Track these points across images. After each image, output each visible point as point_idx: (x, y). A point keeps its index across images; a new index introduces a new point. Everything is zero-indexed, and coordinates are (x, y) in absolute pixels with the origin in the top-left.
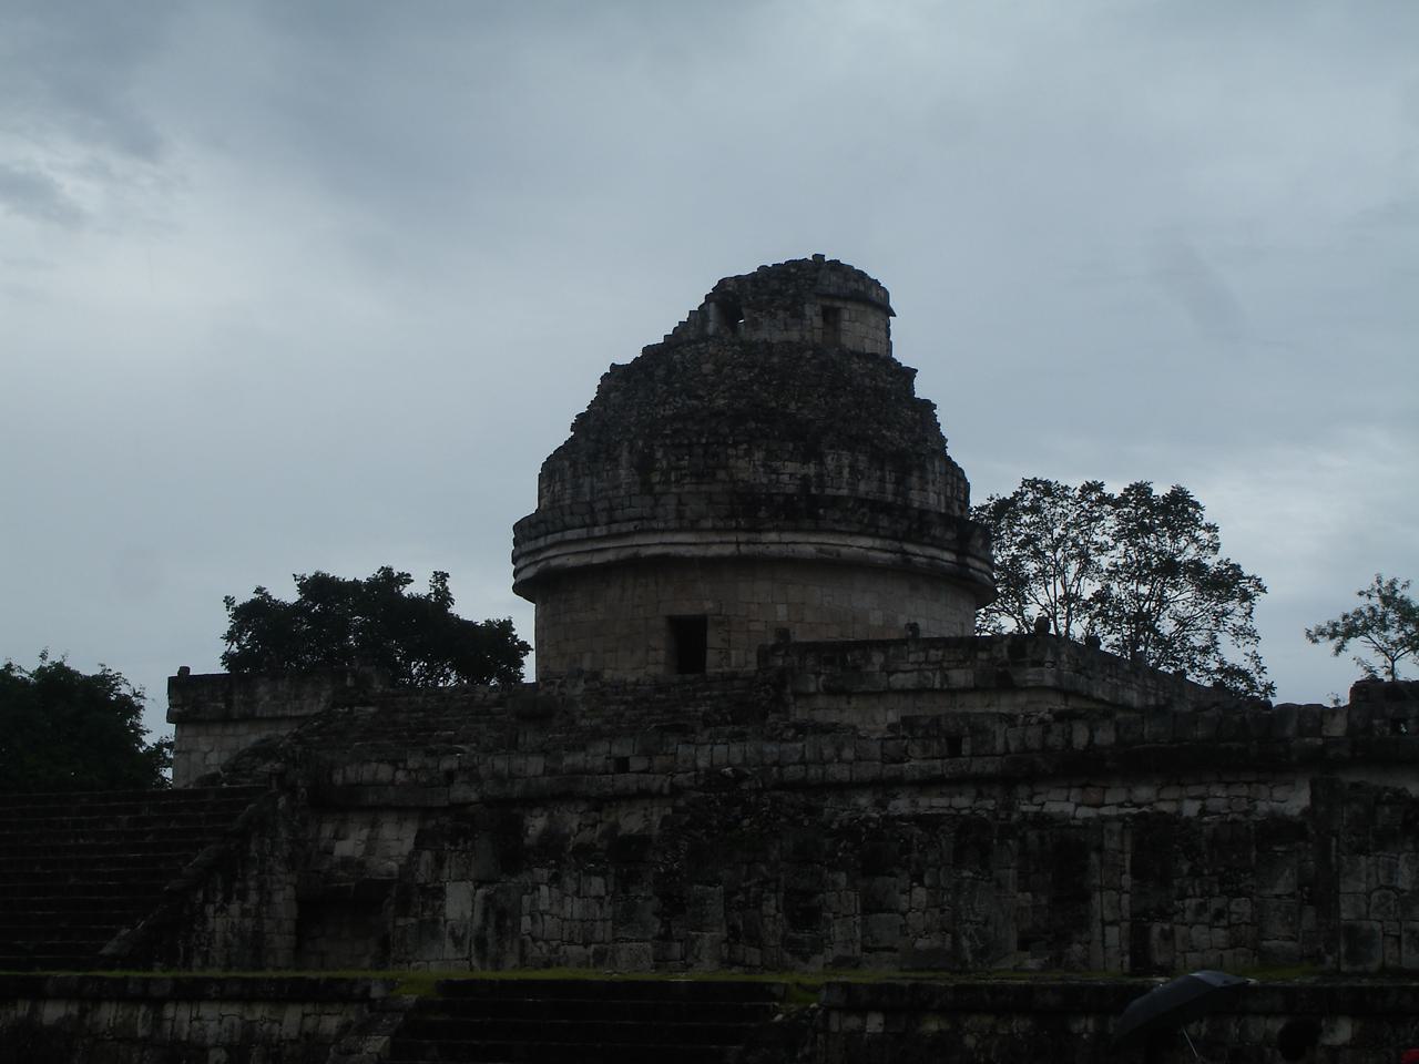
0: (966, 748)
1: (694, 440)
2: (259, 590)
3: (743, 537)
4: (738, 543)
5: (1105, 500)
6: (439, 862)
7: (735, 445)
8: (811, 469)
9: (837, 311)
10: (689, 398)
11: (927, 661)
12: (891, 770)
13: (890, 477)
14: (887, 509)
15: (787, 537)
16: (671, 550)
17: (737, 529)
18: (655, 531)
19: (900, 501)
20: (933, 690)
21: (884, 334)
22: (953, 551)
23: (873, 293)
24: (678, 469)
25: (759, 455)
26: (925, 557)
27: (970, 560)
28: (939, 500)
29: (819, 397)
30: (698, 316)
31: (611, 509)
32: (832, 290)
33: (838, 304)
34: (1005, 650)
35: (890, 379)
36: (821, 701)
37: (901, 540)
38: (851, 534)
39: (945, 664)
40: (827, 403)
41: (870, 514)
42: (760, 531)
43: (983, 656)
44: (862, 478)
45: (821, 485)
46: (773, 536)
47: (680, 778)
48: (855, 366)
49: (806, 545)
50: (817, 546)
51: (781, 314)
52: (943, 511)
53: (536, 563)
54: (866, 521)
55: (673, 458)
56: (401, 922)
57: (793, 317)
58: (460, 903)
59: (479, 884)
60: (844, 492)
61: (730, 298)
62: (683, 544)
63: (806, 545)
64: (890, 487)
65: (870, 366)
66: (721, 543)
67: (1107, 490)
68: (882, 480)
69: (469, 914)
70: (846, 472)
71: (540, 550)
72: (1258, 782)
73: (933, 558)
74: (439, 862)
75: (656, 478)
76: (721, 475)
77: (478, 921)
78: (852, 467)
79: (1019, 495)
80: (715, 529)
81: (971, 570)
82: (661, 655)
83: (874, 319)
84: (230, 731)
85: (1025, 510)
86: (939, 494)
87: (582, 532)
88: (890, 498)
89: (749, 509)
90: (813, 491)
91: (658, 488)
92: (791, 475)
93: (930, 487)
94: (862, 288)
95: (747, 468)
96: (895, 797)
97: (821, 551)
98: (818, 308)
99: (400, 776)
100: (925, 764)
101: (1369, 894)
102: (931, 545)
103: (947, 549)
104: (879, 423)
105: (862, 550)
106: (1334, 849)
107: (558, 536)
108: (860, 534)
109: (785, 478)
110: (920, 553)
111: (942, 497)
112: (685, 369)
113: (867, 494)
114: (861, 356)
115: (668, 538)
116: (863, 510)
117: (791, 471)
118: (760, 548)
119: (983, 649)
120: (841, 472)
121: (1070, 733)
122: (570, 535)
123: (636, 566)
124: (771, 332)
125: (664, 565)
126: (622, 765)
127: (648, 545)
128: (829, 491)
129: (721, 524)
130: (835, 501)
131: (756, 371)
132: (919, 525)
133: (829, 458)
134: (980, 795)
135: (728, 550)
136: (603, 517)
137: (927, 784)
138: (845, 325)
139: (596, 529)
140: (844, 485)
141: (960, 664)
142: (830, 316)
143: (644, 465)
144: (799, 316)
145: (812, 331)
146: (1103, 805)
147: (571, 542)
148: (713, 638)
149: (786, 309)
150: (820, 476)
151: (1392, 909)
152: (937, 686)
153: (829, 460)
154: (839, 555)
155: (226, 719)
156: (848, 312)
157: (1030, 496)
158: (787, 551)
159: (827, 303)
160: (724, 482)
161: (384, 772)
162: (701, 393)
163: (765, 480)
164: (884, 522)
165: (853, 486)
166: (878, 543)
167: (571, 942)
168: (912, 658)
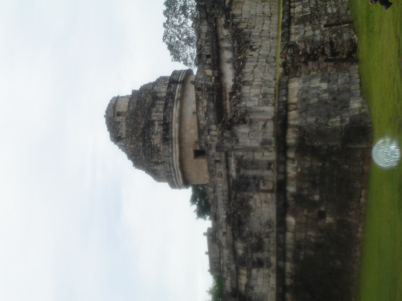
0: (218, 159)
1: (150, 152)
2: (194, 212)
3: (174, 142)
4: (175, 143)
5: (168, 22)
7: (151, 143)
8: (157, 123)
9: (118, 113)
10: (140, 151)
11: (202, 111)
13: (158, 102)
14: (166, 104)
15: (173, 131)
16: (178, 158)
17: (172, 143)
18: (173, 162)
19: (164, 99)
21: (124, 99)
22: (177, 85)
23: (113, 102)
24: (157, 157)
25: (153, 137)
26: (178, 93)
27: (179, 80)
28: (164, 88)
29: (139, 119)
30: (120, 147)
31: (168, 172)
32: (112, 114)
33: (116, 112)
34: (199, 92)
35: (134, 98)
37: (174, 101)
38: (172, 114)
39: (203, 106)
40: (140, 118)
41: (167, 108)
43: (200, 97)
44: (159, 109)
45: (160, 121)
46: (173, 134)
48: (131, 108)
51: (119, 127)
52: (167, 86)
54: (169, 110)
55: (155, 157)
57: (119, 124)
60: (162, 114)
61: (116, 138)
63: (175, 126)
64: (161, 102)
65: (131, 104)
66: (175, 147)
67: (165, 22)
68: (159, 104)
70: (157, 114)
72: (225, 91)
73: (178, 92)
75: (160, 161)
76: (159, 146)
78: (157, 112)
79: (167, 43)
80: (172, 148)
81: (182, 80)
83: (120, 102)
85: (170, 41)
86: (163, 88)
88: (164, 102)
89: (166, 139)
90: (162, 123)
92: (158, 128)
93: (161, 90)
94: (112, 106)
95: (157, 140)
96: (231, 175)
97: (177, 122)
98: (117, 118)
101: (251, 139)
102: (175, 92)
103: (176, 87)
104: (145, 103)
106: (237, 147)
109: (159, 130)
110: (177, 95)
111: (164, 87)
112: (133, 151)
113: (162, 108)
114: (129, 107)
116: (167, 111)
117: (158, 128)
118: (177, 138)
119: (199, 97)
120: (157, 115)
121: (213, 135)
123: (182, 166)
124: (123, 130)
125: (181, 160)
126: (225, 233)
127: (176, 164)
128: (162, 119)
129: (171, 147)
130: (165, 119)
131: (133, 134)
132: (170, 95)
135: (177, 145)
136: (170, 174)
137: (228, 168)
139: (173, 175)
141: (202, 103)
142: (119, 114)
143: (157, 163)
145: (123, 119)
149: (118, 125)
150: (158, 121)
151: (255, 134)
153: (154, 118)
154: (178, 117)
156: (118, 109)
157: (167, 40)
159: (116, 115)
160: (160, 145)
162: (139, 148)
163: (160, 135)
164: (169, 105)
165: (161, 112)
166: (175, 107)
167: (269, 282)
168: (201, 114)
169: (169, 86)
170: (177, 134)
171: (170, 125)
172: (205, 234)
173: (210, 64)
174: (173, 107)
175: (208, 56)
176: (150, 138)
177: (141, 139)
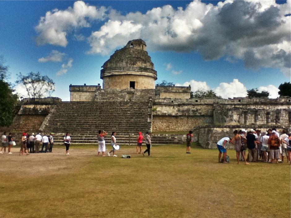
0: (241, 101)
3: (140, 72)
6: (232, 113)
8: (145, 65)
10: (130, 55)
12: (233, 103)
17: (140, 71)
20: (177, 92)
25: (141, 63)
36: (163, 93)
46: (143, 73)
47: (205, 103)
49: (146, 74)
53: (110, 74)
56: (227, 119)
58: (235, 117)
59: (238, 115)
62: (133, 73)
63: (146, 74)
69: (237, 118)
71: (111, 72)
74: (232, 113)
75: (128, 64)
76: (136, 65)
77: (238, 119)
80: (137, 71)
82: (129, 86)
84: (79, 92)
87: (119, 70)
89: (141, 69)
91: (129, 66)
99: (165, 101)
100: (237, 102)
107: (115, 71)
108: (151, 73)
115: (131, 72)
117: (143, 65)
122: (116, 70)
126: (197, 101)
128: (147, 68)
130: (149, 69)
134: (243, 106)
135: (139, 74)
136: (122, 69)
138: (144, 48)
142: (143, 46)
143: (127, 63)
144: (140, 46)
146: (257, 107)
147: (117, 71)
148: (136, 84)
152: (178, 92)
155: (79, 91)
158: (145, 74)
161: (163, 101)
164: (153, 71)
170: (143, 74)
171: (147, 71)
173: (286, 101)
175: (290, 101)
176: (140, 60)
177: (136, 56)
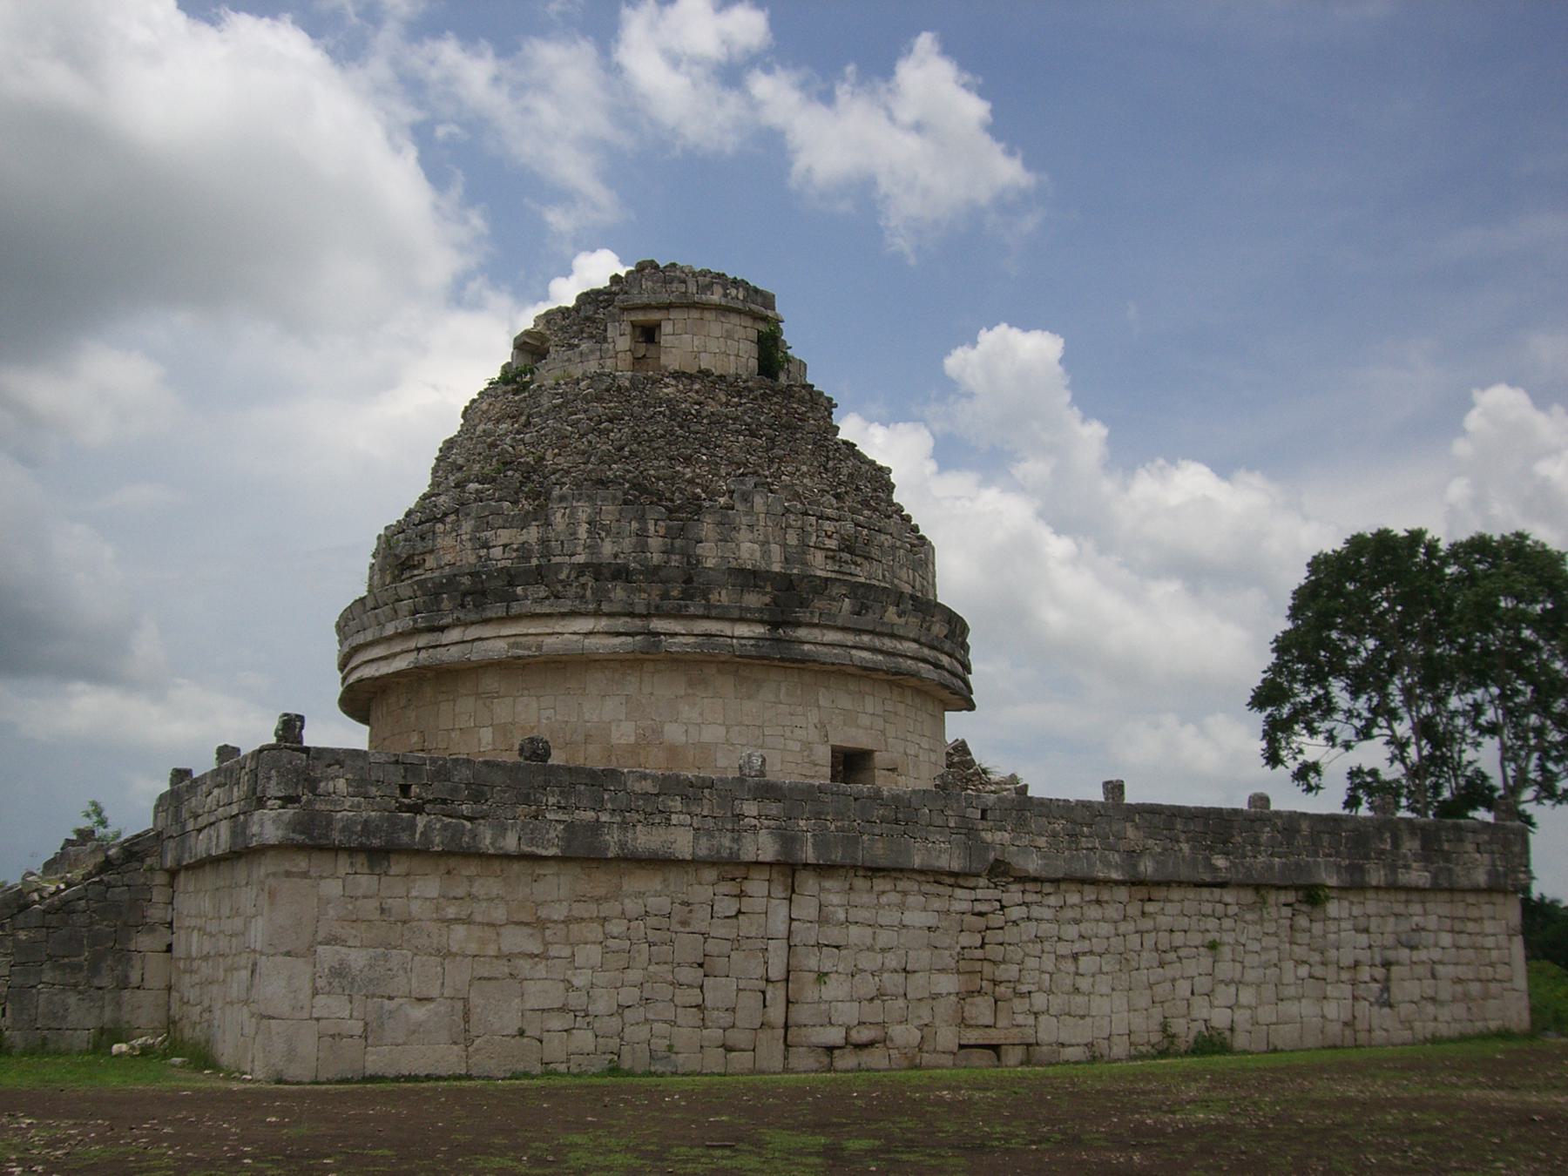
8: (532, 534)
14: (621, 574)
22: (761, 622)
38: (563, 615)
42: (442, 629)
50: (512, 640)
52: (776, 568)
63: (495, 641)
70: (582, 531)
92: (505, 546)
93: (744, 534)
105: (575, 637)
113: (616, 556)
128: (555, 560)
133: (559, 515)
140: (579, 549)
150: (544, 542)
164: (619, 593)
166: (603, 624)
169: (749, 578)
172: (1114, 789)
174: (597, 614)
